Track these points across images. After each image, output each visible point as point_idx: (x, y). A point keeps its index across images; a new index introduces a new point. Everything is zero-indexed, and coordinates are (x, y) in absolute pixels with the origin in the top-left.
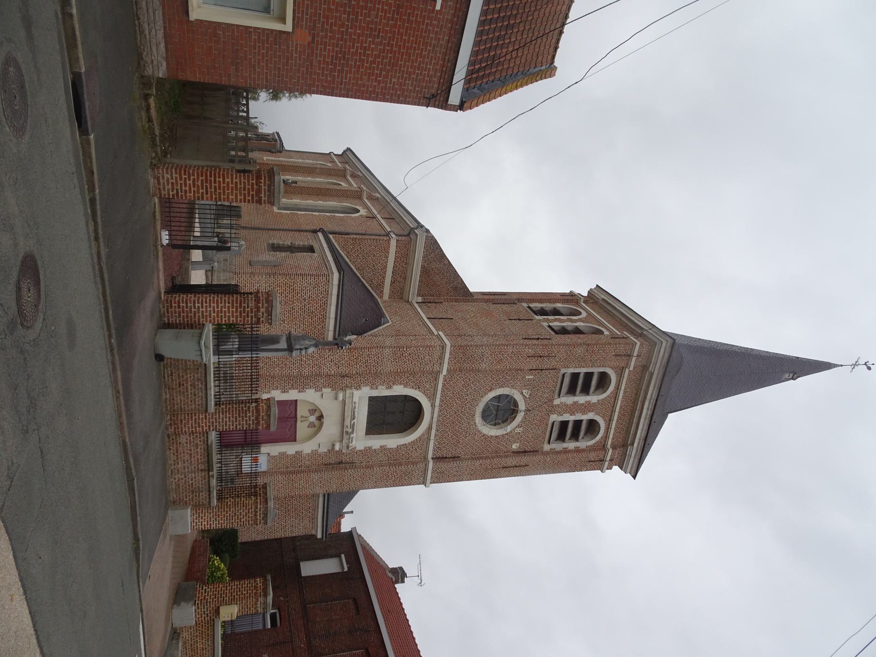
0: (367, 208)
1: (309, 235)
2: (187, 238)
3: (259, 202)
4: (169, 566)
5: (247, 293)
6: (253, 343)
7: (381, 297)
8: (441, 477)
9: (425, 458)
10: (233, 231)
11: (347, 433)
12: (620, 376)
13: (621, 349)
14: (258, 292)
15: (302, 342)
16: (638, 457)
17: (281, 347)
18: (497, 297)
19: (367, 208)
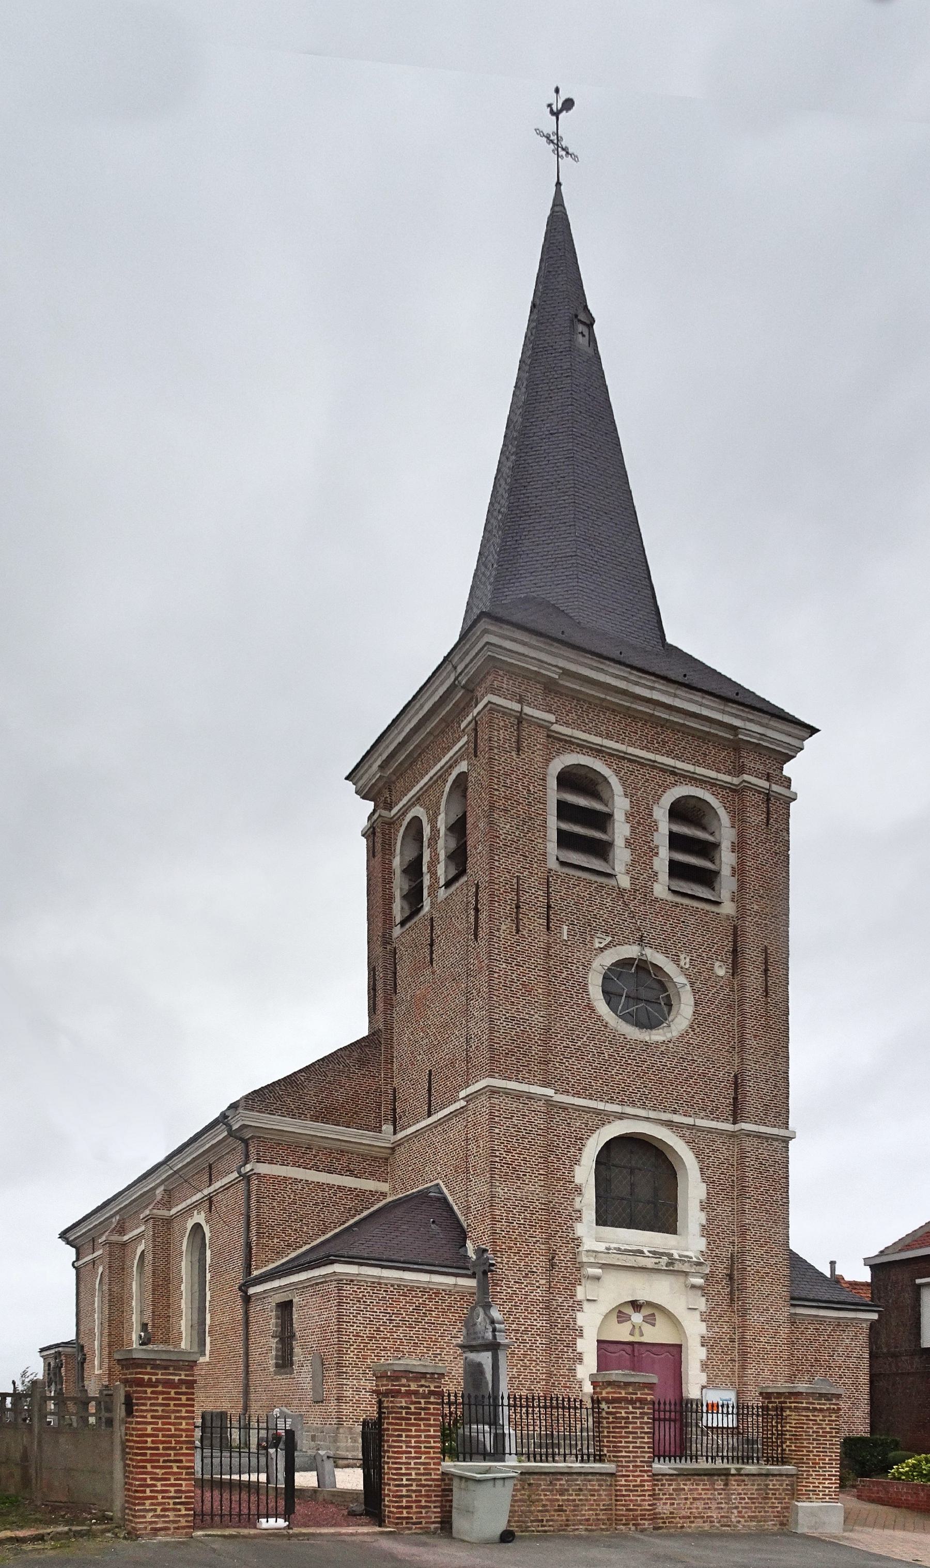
0: (189, 1210)
1: (255, 1308)
2: (272, 1494)
3: (191, 1384)
4: (899, 1534)
5: (380, 1408)
6: (480, 1401)
7: (384, 1195)
8: (778, 1107)
9: (732, 1135)
10: (254, 1424)
11: (668, 1265)
12: (569, 744)
13: (503, 735)
14: (377, 1392)
15: (479, 1327)
16: (765, 719)
17: (490, 1361)
18: (380, 985)
19: (189, 1210)
